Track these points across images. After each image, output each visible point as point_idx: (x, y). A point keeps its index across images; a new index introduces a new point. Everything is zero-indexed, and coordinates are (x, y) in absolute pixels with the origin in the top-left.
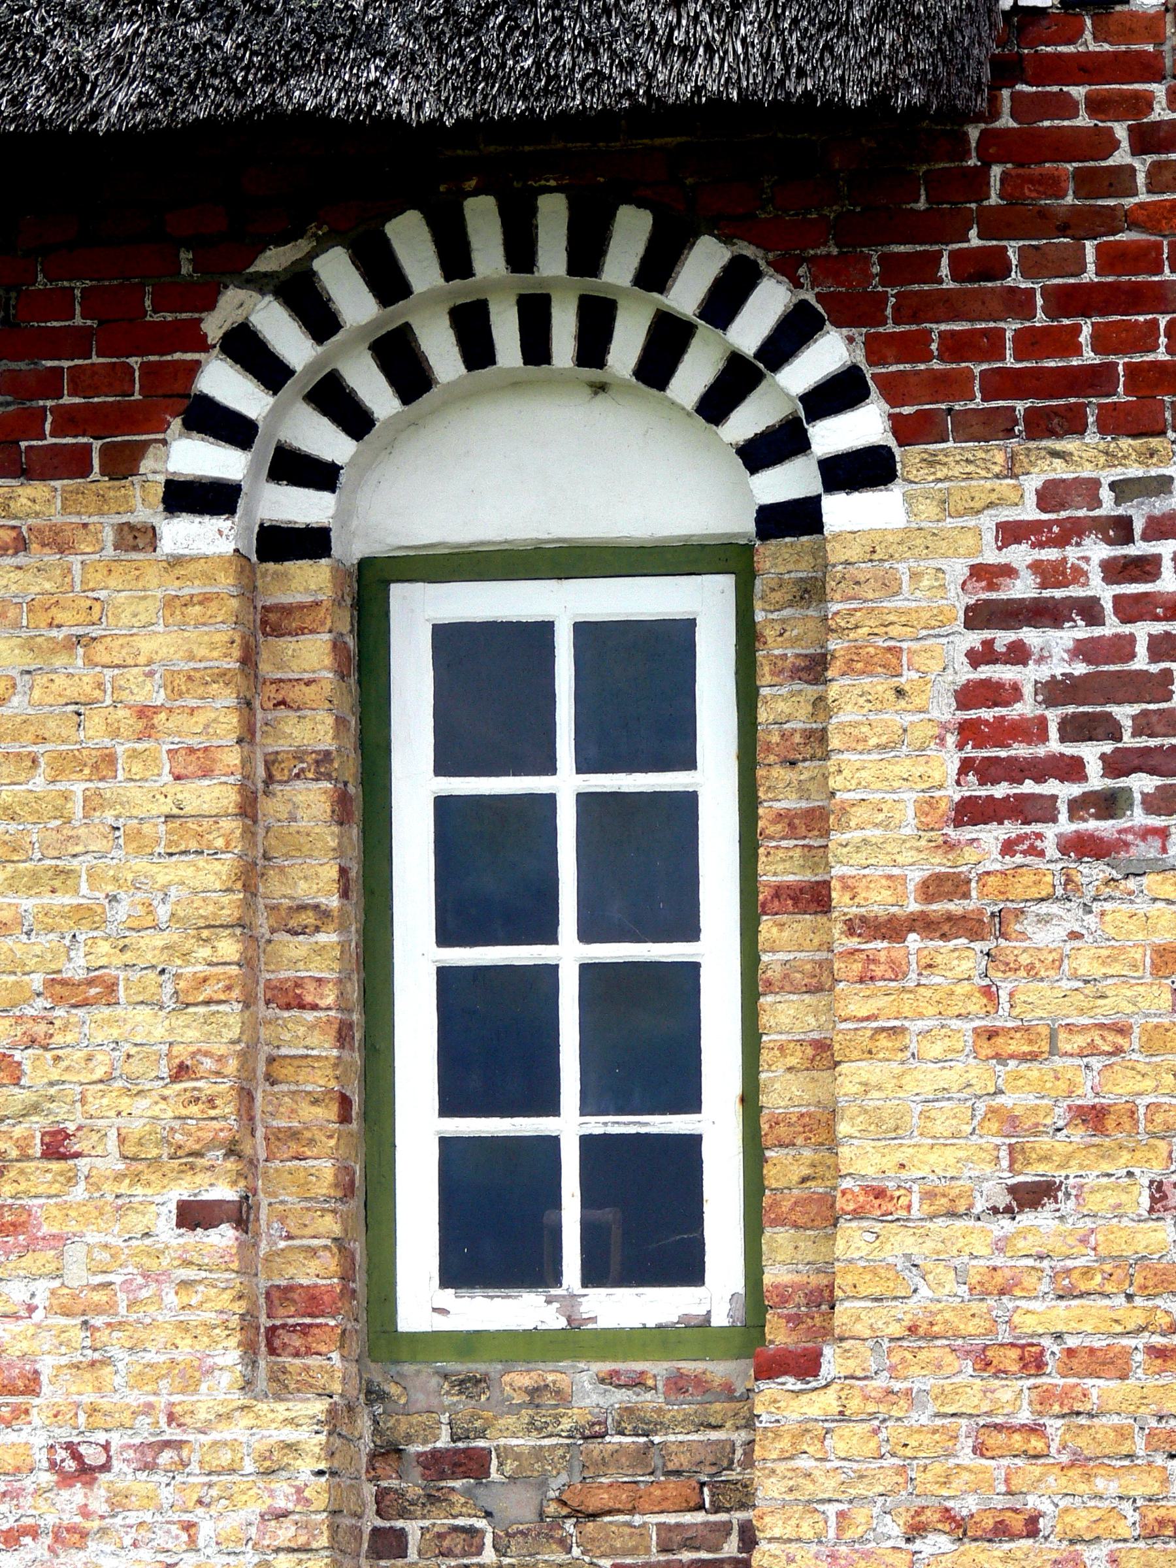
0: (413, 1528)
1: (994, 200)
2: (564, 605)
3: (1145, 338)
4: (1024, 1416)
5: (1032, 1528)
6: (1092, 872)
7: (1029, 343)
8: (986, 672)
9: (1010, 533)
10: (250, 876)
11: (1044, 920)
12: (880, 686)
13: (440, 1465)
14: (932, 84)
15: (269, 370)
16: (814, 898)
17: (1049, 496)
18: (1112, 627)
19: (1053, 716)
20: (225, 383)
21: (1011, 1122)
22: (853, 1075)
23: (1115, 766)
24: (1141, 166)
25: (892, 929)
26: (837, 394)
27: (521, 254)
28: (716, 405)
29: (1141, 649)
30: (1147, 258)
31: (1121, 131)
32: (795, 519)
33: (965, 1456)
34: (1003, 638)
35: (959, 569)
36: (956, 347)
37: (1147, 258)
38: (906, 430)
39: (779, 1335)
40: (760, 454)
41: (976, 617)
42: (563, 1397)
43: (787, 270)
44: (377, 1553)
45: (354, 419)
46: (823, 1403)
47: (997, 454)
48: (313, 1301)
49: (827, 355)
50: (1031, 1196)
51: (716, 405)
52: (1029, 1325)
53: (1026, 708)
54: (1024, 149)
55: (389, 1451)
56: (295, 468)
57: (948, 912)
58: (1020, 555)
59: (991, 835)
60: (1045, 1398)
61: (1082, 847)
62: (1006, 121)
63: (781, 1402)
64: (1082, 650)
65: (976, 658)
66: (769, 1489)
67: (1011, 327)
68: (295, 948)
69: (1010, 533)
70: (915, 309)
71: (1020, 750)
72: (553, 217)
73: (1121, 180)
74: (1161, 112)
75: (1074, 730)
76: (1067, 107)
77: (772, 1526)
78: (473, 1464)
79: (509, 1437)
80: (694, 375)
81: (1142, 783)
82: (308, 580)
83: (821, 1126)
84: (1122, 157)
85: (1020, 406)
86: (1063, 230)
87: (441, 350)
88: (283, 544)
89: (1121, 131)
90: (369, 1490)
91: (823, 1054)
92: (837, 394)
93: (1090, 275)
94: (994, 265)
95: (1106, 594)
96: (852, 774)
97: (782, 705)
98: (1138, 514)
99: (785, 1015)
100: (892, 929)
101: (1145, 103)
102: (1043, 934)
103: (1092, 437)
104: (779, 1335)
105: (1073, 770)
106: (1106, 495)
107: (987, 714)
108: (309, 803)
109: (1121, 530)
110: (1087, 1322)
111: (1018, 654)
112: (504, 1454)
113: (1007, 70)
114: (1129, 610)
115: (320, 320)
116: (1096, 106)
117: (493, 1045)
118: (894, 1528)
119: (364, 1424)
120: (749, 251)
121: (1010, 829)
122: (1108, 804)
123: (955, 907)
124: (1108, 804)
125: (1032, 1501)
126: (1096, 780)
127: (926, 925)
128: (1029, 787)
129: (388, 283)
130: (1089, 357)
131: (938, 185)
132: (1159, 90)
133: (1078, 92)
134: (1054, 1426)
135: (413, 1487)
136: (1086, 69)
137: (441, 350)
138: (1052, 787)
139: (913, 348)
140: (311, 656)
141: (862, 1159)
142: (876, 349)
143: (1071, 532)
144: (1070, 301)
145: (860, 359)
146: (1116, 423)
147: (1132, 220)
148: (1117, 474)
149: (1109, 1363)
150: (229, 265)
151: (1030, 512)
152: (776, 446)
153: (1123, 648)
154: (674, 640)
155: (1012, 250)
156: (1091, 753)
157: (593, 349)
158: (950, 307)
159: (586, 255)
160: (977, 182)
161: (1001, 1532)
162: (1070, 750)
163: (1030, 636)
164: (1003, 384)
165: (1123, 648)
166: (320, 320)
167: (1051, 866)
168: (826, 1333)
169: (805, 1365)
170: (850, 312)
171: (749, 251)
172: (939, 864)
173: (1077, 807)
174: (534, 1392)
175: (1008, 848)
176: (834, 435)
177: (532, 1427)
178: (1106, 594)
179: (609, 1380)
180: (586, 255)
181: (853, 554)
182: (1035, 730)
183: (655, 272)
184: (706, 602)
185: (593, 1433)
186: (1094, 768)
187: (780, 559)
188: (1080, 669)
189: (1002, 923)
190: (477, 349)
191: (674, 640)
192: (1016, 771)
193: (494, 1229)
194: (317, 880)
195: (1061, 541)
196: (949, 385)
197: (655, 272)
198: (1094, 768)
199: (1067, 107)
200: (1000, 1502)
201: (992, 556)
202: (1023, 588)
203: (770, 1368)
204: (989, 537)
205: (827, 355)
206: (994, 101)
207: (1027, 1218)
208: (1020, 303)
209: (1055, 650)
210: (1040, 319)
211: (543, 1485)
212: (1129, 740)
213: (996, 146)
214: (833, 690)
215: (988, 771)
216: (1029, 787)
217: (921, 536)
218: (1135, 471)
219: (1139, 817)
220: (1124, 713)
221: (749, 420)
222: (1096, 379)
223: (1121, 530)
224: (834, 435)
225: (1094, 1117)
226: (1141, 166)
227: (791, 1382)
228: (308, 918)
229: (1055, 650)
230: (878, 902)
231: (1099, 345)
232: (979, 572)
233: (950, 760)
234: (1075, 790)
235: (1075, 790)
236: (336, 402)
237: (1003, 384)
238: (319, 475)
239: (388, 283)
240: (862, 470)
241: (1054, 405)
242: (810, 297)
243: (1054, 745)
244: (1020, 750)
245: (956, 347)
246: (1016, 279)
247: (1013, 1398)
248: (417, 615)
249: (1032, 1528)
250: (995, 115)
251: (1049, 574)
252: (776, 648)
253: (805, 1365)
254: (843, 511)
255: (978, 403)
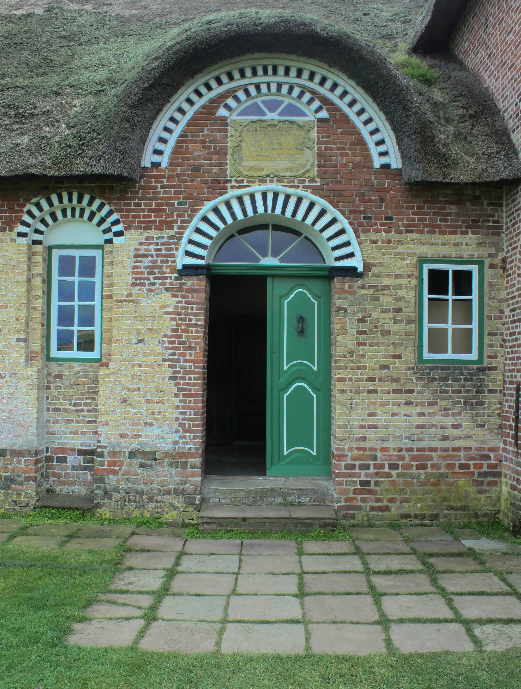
0: (52, 385)
1: (140, 195)
2: (78, 253)
3: (161, 216)
4: (139, 374)
5: (139, 390)
6: (151, 294)
7: (145, 216)
8: (136, 264)
9: (141, 244)
10: (29, 291)
11: (144, 301)
12: (120, 266)
13: (56, 377)
14: (129, 173)
15: (33, 217)
16: (110, 297)
17: (147, 239)
18: (155, 258)
19: (146, 271)
20: (26, 218)
21: (138, 330)
22: (115, 323)
23: (155, 278)
24: (162, 191)
25: (121, 301)
26: (116, 222)
27: (70, 200)
28: (99, 224)
29: (159, 262)
30: (162, 204)
31: (159, 186)
32: (109, 241)
33: (130, 379)
34: (139, 259)
35: (133, 249)
36: (134, 216)
37: (162, 204)
38: (126, 228)
39: (104, 360)
40: (105, 232)
41: (136, 256)
42: (74, 367)
43: (109, 204)
44: (47, 389)
45: (47, 225)
46: (108, 371)
47: (139, 232)
48: (37, 353)
49: (115, 216)
50: (140, 341)
51: (99, 224)
52: (140, 360)
53: (142, 270)
54: (145, 188)
55: (49, 374)
56: (37, 231)
57: (129, 299)
58: (142, 247)
59: (136, 288)
60: (142, 371)
61: (150, 290)
62: (142, 184)
63: (103, 370)
64: (151, 261)
65: (135, 262)
66: (101, 382)
67: (142, 214)
68: (35, 301)
69: (141, 244)
70: (127, 211)
71: (141, 276)
72: (75, 196)
73: (158, 193)
74: (165, 183)
75: (149, 273)
76: (151, 182)
77: (102, 389)
78: (61, 377)
79: (66, 373)
80: (96, 219)
81: (158, 281)
82: (39, 248)
83: (110, 330)
84: (159, 189)
85: (143, 225)
86: (150, 200)
87: (59, 215)
88: (35, 242)
89: (159, 186)
90: (46, 380)
91: (111, 320)
92: (116, 222)
93: (154, 207)
94: (139, 205)
95: (154, 253)
96: (116, 279)
97: (107, 268)
98: (160, 241)
99: (106, 313)
100: (121, 301)
101: (163, 181)
102: (144, 302)
103: (153, 230)
104: (104, 360)
105: (148, 279)
106: (155, 239)
107: (136, 270)
108: (38, 281)
109: (157, 244)
110: (148, 360)
111: (141, 262)
112: (66, 375)
113: (142, 176)
114: (158, 256)
115: (41, 209)
116: (155, 182)
117: (66, 316)
118: (119, 389)
119: (45, 371)
120: (104, 201)
121: (139, 287)
122: (153, 284)
123: (130, 298)
124: (153, 284)
125: (139, 386)
126: (152, 281)
127: (126, 301)
128: (142, 281)
129: (51, 204)
130: (153, 219)
131: (132, 192)
132: (165, 180)
133: (153, 180)
134: (143, 375)
135: (52, 379)
136: (154, 176)
137: (59, 215)
138: (145, 281)
139: (127, 216)
140: (39, 259)
141: (116, 335)
142: (122, 216)
143: (150, 244)
144: (150, 210)
145: (119, 217)
146: (157, 228)
147: (160, 199)
148: (157, 236)
149: (151, 366)
150: (28, 200)
151: (144, 241)
152: (107, 231)
153: (156, 261)
154: (93, 259)
155: (142, 202)
156: (151, 277)
157: (81, 216)
158: (133, 210)
159: (80, 201)
160: (137, 192)
161: (135, 390)
162: (148, 276)
163: (143, 259)
164: (140, 222)
165: (156, 261)
166: (41, 209)
167: (145, 293)
168: (110, 360)
169: (107, 365)
170: (119, 211)
171: (104, 201)
172: (129, 292)
173: (149, 284)
174: (70, 366)
175: (139, 290)
176: (115, 229)
177: (69, 372)
178: (154, 253)
179: (81, 365)
180: (80, 201)
181: (117, 246)
182: (143, 273)
183: (90, 204)
184: (97, 253)
185: (78, 373)
186: (152, 279)
187: (108, 247)
188: (150, 264)
189: (137, 301)
190: (65, 215)
191: (93, 259)
192: (140, 279)
193: (65, 343)
194: (38, 291)
195: (148, 245)
196: (133, 222)
197: (90, 204)
198: (152, 279)
199: (151, 182)
200: (135, 386)
201: (138, 247)
202: (142, 252)
203: (102, 365)
204: (137, 244)
205: (115, 216)
206: (140, 180)
207: (140, 345)
208: (143, 210)
209: (146, 261)
210: (146, 213)
211: (71, 380)
212: (157, 275)
213: (140, 187)
214: (114, 266)
215: (136, 279)
216: (142, 281)
217: (129, 243)
218: (159, 236)
219: (158, 286)
220: (156, 271)
221: (104, 226)
222: (154, 222)
223: (157, 244)
224: (115, 229)
225: (150, 330)
226: (162, 191)
227: (104, 368)
228: (37, 297)
229: (146, 261)
230: (120, 298)
231: (155, 217)
232: (136, 249)
233: (130, 277)
234: (149, 282)
235: (149, 282)
236: (43, 221)
237: (140, 222)
238: (42, 233)
239: (51, 204)
240: (119, 234)
241: (147, 225)
242: (112, 208)
243: (146, 275)
244: (141, 276)
245: (134, 216)
246: (143, 207)
247: (137, 371)
248: (56, 254)
249: (139, 390)
250: (140, 182)
251: (146, 250)
252: (107, 260)
253: (107, 365)
254: (116, 240)
255: (137, 225)
